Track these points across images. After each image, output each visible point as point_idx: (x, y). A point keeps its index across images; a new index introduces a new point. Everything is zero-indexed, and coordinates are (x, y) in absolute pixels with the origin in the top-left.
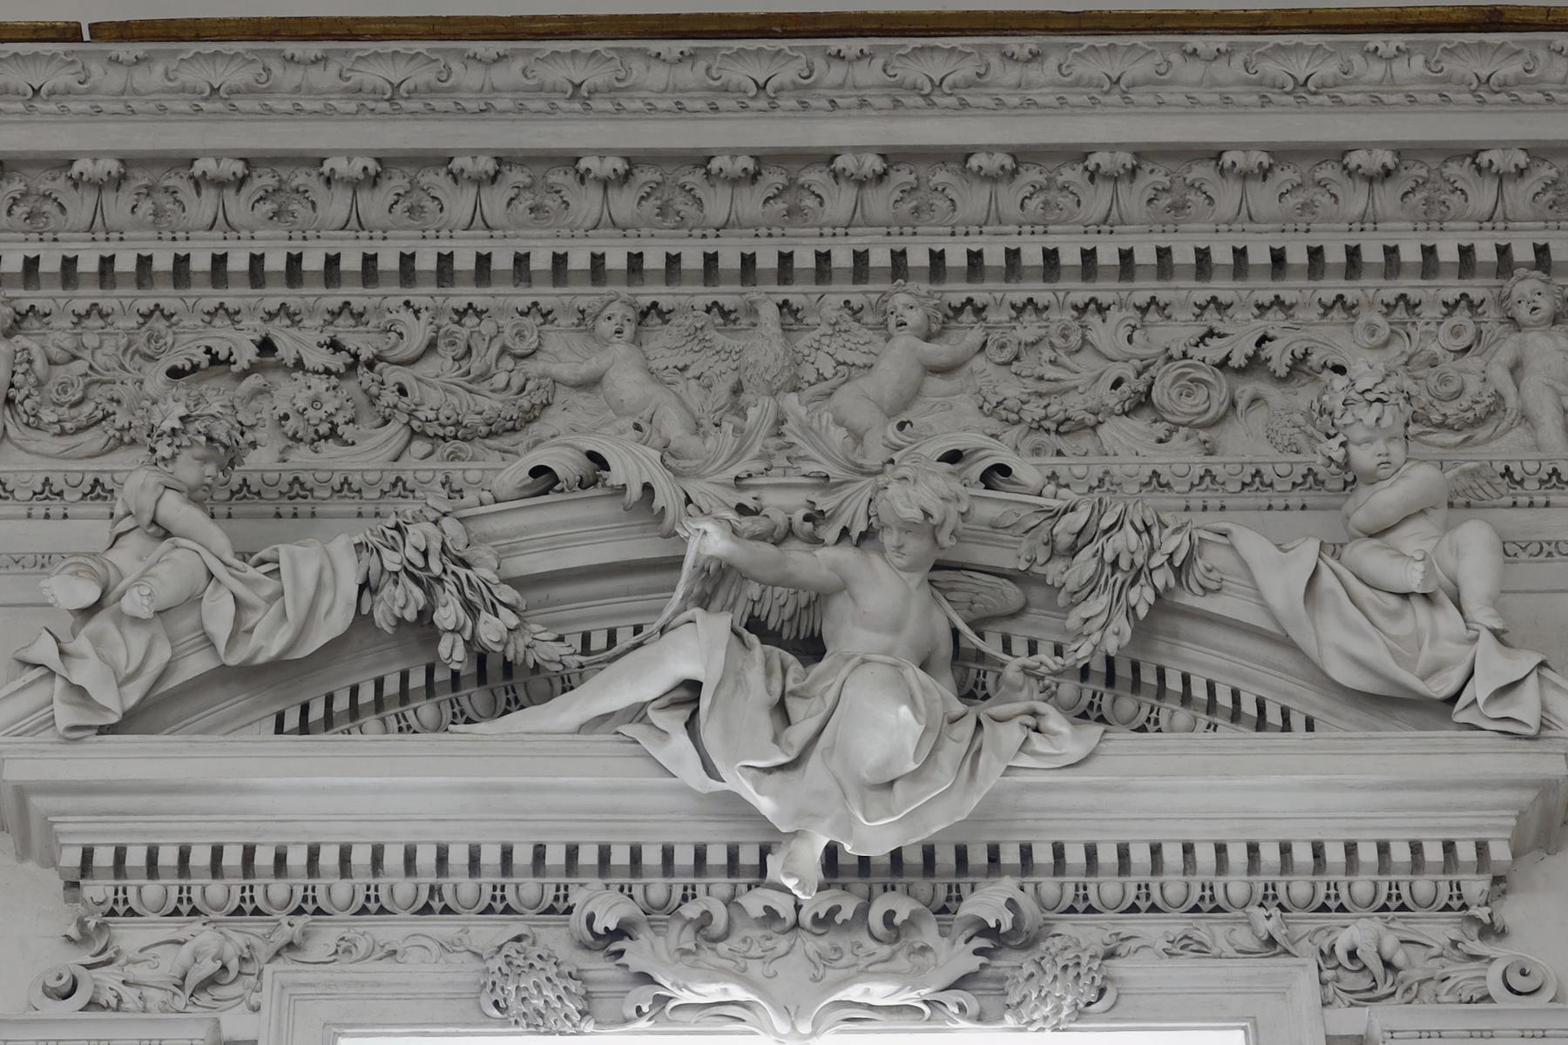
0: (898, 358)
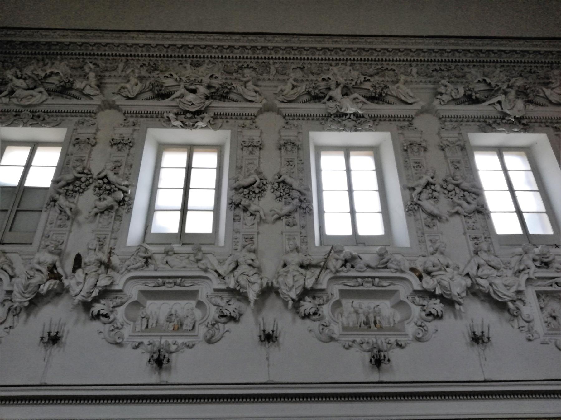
0: (498, 70)
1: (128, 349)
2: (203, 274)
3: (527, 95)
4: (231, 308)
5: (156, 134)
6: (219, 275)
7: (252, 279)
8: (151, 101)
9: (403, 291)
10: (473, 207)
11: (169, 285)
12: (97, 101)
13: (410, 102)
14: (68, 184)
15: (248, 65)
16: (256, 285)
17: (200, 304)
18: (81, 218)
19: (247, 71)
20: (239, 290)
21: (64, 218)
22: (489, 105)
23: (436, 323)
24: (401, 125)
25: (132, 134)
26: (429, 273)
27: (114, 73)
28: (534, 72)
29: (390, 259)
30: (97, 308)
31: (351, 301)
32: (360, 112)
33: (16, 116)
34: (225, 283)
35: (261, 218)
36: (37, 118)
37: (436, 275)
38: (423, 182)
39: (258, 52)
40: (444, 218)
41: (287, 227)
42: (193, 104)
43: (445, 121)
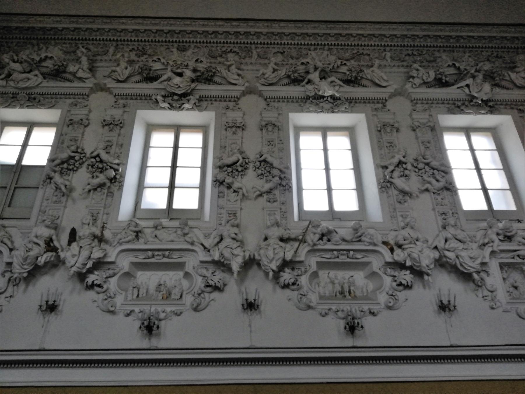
0: (467, 54)
1: (121, 316)
2: (190, 247)
3: (493, 78)
4: (216, 279)
5: (145, 115)
6: (205, 248)
7: (235, 252)
8: (140, 84)
9: (376, 263)
10: (441, 184)
11: (158, 257)
12: (89, 84)
13: (384, 85)
14: (63, 163)
15: (231, 50)
16: (239, 257)
17: (187, 275)
18: (75, 195)
19: (230, 56)
20: (223, 262)
21: (60, 194)
22: (458, 88)
23: (407, 292)
24: (376, 107)
25: (122, 115)
26: (400, 246)
27: (105, 57)
28: (501, 57)
29: (364, 233)
30: (91, 278)
31: (327, 272)
32: (337, 95)
33: (13, 98)
34: (211, 256)
35: (243, 195)
36: (33, 100)
37: (407, 248)
38: (396, 161)
39: (241, 37)
40: (414, 195)
41: (268, 204)
42: (179, 87)
43: (417, 103)
